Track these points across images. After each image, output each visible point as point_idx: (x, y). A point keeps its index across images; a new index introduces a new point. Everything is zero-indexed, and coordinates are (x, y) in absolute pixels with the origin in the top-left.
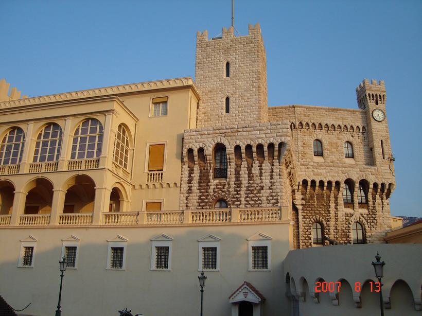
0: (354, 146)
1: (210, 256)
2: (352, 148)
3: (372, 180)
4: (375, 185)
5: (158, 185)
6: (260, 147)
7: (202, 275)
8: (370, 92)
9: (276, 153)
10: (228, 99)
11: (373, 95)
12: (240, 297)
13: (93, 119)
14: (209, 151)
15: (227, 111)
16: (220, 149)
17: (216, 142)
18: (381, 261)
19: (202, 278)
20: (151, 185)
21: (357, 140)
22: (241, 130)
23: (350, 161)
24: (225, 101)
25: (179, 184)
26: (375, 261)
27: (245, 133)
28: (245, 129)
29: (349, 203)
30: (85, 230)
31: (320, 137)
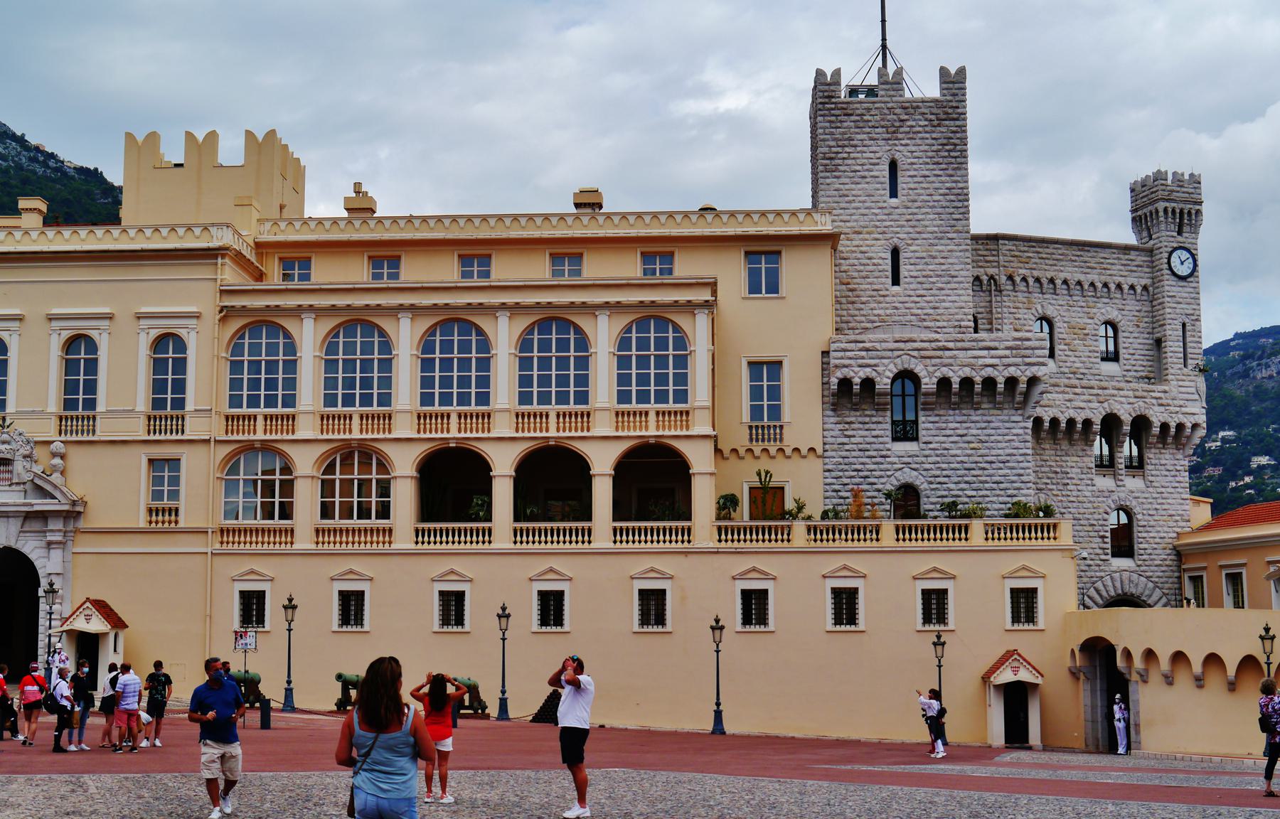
0: (1121, 334)
2: (1116, 337)
3: (1157, 416)
4: (1165, 427)
5: (773, 451)
6: (989, 383)
7: (939, 637)
8: (1167, 204)
9: (1019, 398)
10: (895, 253)
11: (1174, 211)
13: (656, 318)
15: (896, 281)
17: (900, 367)
18: (1271, 633)
19: (939, 643)
20: (757, 451)
21: (1126, 312)
22: (951, 345)
23: (1110, 368)
24: (889, 255)
25: (820, 451)
26: (1263, 633)
28: (959, 345)
29: (1106, 465)
30: (682, 557)
31: (1050, 312)
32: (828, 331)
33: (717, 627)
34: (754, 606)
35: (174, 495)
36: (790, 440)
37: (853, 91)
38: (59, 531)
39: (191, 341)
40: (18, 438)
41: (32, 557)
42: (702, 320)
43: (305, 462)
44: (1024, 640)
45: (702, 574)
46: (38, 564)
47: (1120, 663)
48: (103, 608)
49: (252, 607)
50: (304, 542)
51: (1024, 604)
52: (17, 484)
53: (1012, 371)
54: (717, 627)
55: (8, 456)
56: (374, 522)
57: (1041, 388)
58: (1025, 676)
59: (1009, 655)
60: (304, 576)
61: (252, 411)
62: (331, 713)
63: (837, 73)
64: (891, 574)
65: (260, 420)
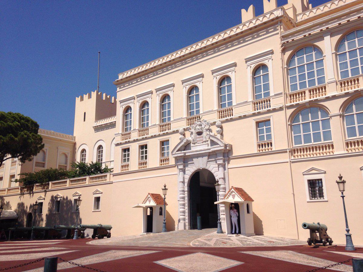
35: (269, 137)
38: (221, 159)
39: (269, 63)
40: (204, 123)
41: (213, 171)
43: (334, 107)
46: (215, 175)
49: (315, 188)
52: (205, 142)
55: (201, 131)
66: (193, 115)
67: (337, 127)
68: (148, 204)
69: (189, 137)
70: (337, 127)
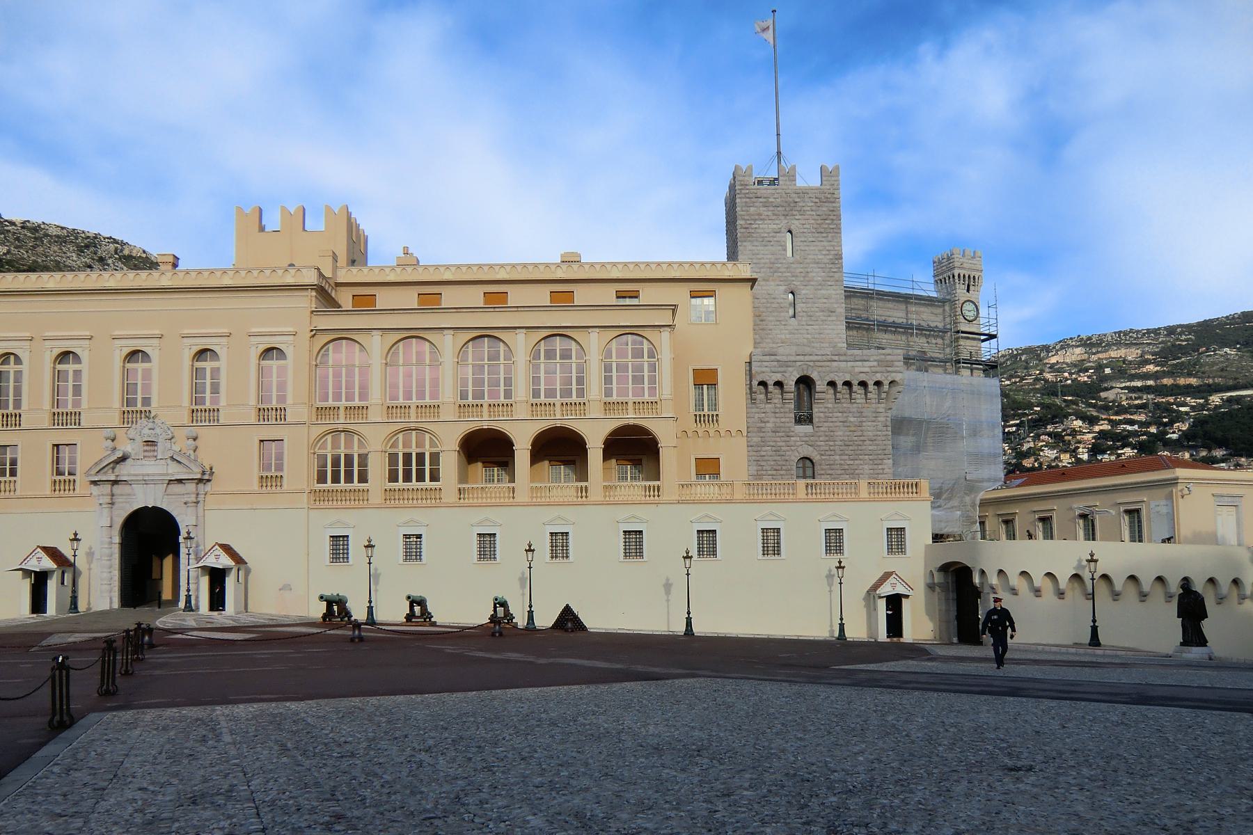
1: (834, 540)
5: (712, 432)
6: (863, 384)
7: (840, 562)
12: (887, 589)
14: (790, 385)
16: (805, 382)
22: (836, 358)
27: (843, 364)
28: (842, 358)
32: (750, 349)
33: (688, 557)
34: (707, 541)
36: (723, 425)
37: (760, 183)
39: (289, 351)
41: (174, 514)
42: (666, 334)
44: (895, 563)
45: (669, 518)
47: (977, 580)
48: (227, 549)
49: (339, 546)
50: (376, 497)
51: (896, 539)
53: (878, 377)
54: (688, 557)
56: (428, 483)
57: (899, 388)
58: (900, 590)
59: (887, 576)
60: (376, 521)
61: (336, 404)
62: (401, 625)
63: (750, 168)
64: (803, 519)
65: (342, 410)
66: (134, 408)
67: (377, 468)
68: (34, 565)
69: (125, 447)
70: (377, 468)
